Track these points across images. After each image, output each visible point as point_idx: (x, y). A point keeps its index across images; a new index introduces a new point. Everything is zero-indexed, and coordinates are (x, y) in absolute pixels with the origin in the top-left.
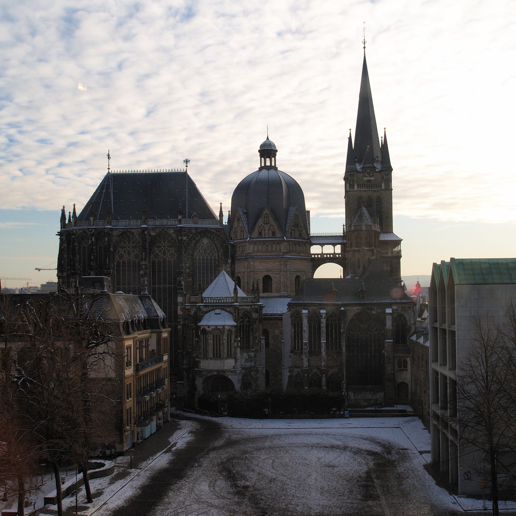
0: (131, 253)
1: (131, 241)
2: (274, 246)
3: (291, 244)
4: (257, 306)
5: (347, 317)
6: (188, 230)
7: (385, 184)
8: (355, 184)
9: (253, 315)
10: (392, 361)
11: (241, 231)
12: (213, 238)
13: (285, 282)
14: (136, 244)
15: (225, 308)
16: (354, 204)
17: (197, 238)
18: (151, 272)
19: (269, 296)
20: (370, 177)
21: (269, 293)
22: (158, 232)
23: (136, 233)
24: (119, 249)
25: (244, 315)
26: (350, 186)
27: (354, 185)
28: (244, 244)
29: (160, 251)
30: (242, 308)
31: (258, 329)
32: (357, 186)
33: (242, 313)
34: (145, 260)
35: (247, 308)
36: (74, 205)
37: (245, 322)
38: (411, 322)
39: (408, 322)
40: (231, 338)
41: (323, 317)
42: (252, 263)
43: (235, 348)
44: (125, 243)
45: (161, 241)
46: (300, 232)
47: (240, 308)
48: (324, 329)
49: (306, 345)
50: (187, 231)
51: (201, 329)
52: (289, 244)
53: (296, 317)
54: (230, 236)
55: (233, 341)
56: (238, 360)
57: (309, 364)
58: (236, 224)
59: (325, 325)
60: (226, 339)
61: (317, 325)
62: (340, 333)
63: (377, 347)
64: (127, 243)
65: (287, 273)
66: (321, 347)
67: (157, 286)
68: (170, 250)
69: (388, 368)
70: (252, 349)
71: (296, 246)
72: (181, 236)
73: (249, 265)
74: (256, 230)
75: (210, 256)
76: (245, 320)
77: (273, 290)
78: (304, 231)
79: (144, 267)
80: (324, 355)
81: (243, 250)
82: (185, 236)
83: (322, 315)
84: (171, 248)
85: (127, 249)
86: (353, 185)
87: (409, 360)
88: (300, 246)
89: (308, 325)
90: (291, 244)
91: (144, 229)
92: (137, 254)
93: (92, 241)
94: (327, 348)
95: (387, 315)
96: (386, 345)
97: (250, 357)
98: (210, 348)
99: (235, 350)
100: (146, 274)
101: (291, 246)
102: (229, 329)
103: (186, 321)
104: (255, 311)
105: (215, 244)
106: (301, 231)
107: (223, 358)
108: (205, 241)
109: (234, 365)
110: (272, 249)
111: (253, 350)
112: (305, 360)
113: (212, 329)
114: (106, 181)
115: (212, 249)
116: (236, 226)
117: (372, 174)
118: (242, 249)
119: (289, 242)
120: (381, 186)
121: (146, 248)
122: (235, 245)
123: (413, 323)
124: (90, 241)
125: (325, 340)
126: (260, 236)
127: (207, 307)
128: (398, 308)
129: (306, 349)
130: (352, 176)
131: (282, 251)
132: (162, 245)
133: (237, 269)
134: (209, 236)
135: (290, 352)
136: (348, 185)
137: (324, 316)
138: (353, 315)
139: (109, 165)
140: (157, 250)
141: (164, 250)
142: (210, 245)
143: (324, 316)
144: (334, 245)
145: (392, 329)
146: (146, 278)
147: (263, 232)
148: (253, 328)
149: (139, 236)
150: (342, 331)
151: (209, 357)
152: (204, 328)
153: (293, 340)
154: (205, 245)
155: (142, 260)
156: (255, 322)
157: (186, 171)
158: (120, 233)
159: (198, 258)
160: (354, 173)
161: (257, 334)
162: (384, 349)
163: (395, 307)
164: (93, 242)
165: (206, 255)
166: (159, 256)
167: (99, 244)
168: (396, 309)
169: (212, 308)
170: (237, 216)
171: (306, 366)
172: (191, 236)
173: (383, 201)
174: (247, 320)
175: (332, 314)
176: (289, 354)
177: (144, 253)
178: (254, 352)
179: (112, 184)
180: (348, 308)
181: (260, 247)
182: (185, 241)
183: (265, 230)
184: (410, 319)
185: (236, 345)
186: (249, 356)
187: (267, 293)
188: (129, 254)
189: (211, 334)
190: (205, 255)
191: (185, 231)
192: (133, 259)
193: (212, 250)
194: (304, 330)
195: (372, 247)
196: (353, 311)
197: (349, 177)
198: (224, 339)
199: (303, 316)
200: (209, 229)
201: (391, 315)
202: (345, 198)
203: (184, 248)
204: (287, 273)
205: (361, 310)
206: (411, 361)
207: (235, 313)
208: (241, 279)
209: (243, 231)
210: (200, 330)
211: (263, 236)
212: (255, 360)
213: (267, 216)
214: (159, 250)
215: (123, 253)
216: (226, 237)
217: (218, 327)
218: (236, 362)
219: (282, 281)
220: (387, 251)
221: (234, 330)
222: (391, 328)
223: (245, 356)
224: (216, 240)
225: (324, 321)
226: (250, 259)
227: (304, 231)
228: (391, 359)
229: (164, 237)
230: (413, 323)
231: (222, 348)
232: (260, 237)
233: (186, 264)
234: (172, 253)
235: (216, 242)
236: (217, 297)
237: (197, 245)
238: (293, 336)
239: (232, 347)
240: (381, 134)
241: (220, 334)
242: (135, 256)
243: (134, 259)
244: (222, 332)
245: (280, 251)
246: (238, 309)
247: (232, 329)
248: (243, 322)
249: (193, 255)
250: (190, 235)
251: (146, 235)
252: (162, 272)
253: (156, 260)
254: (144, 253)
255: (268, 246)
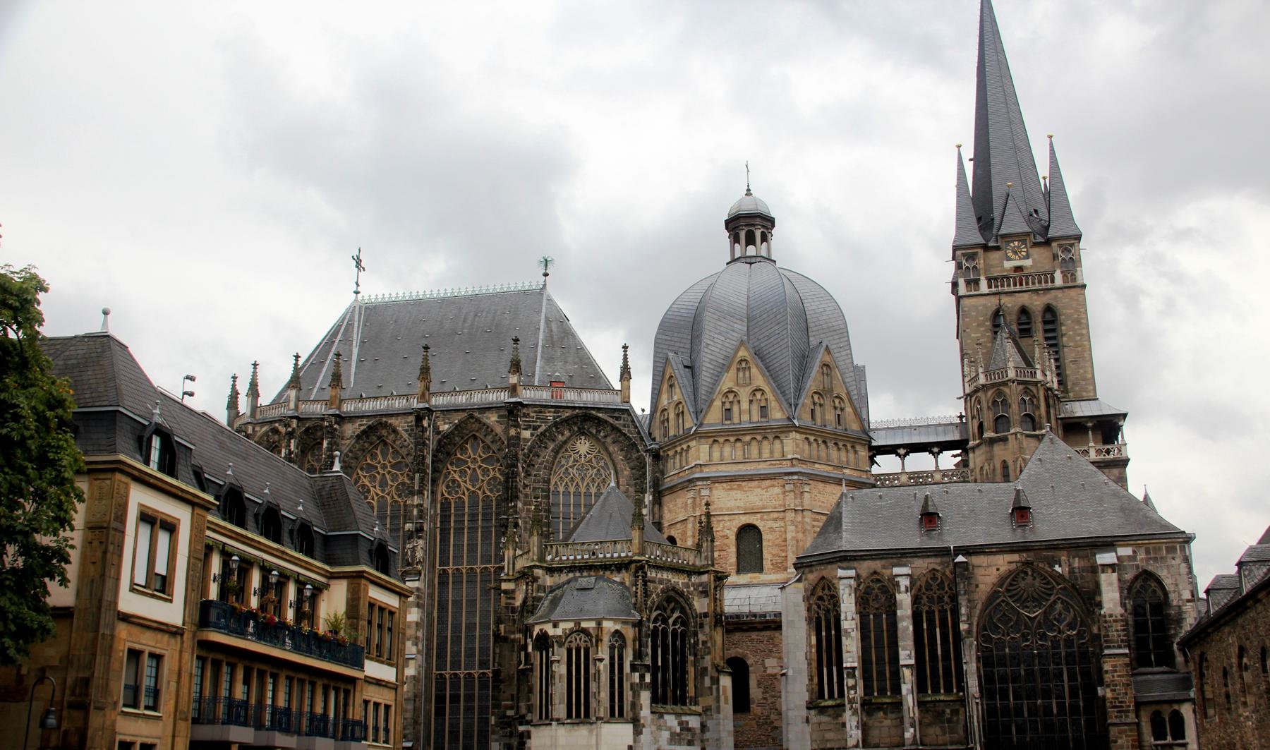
0: (390, 482)
1: (391, 451)
2: (765, 443)
3: (812, 438)
4: (706, 575)
5: (977, 586)
6: (535, 412)
7: (1062, 272)
8: (983, 278)
9: (695, 603)
10: (1132, 718)
11: (678, 415)
12: (605, 437)
13: (797, 541)
14: (403, 458)
15: (608, 573)
16: (982, 329)
17: (560, 437)
18: (438, 531)
19: (755, 581)
20: (1020, 259)
21: (757, 575)
22: (456, 421)
23: (403, 427)
24: (358, 474)
25: (669, 600)
26: (968, 282)
27: (979, 280)
28: (685, 447)
29: (463, 473)
30: (659, 575)
31: (709, 645)
32: (986, 282)
33: (659, 591)
34: (420, 492)
35: (676, 580)
36: (255, 365)
37: (671, 621)
38: (1180, 595)
39: (1172, 596)
40: (621, 658)
41: (903, 588)
42: (705, 492)
43: (636, 689)
44: (374, 456)
45: (467, 449)
46: (840, 413)
47: (654, 575)
48: (905, 624)
49: (854, 676)
50: (532, 414)
51: (535, 634)
52: (807, 438)
53: (820, 598)
54: (650, 434)
55: (627, 668)
56: (644, 726)
57: (864, 740)
58: (664, 401)
59: (909, 612)
60: (607, 661)
61: (884, 616)
62: (958, 637)
63: (1079, 680)
64: (380, 457)
65: (803, 517)
66: (902, 680)
67: (451, 568)
68: (488, 470)
69: (1120, 742)
70: (693, 708)
71: (827, 447)
72: (517, 426)
73: (698, 499)
74: (717, 403)
75: (596, 485)
76: (669, 617)
77: (767, 564)
78: (849, 410)
79: (415, 512)
80: (911, 704)
81: (684, 464)
82: (524, 429)
83: (898, 582)
84: (493, 465)
85: (378, 473)
86: (977, 282)
87: (1187, 711)
88: (839, 449)
89: (857, 617)
90: (812, 438)
91: (419, 415)
92: (403, 484)
93: (290, 450)
94: (921, 687)
95: (1103, 572)
96: (1107, 667)
97: (689, 730)
98: (559, 689)
99: (634, 697)
100: (420, 530)
101: (815, 445)
102: (617, 631)
103: (502, 627)
104: (702, 592)
105: (610, 454)
106: (842, 409)
107: (599, 719)
108: (583, 446)
109: (631, 743)
110: (760, 453)
111: (699, 709)
112: (851, 721)
113: (564, 630)
114: (348, 316)
115: (602, 467)
116: (665, 403)
117: (1027, 252)
118: (680, 461)
119: (806, 433)
120: (1053, 281)
121: (423, 464)
122: (662, 454)
123: (1189, 597)
124: (283, 451)
125: (910, 658)
126: (726, 420)
127: (556, 575)
128: (1134, 552)
129: (855, 690)
130: (971, 257)
131: (790, 457)
132: (469, 457)
133: (668, 518)
134: (594, 432)
135: (808, 708)
136: (961, 282)
137: (904, 582)
138: (995, 580)
139: (358, 285)
140: (455, 471)
141: (474, 469)
142: (595, 457)
143: (904, 582)
144: (934, 448)
145: (1122, 615)
146: (421, 542)
147: (735, 408)
148: (696, 643)
149: (410, 435)
150: (963, 627)
151: (555, 715)
152: (541, 630)
153: (815, 671)
154: (583, 457)
155: (412, 493)
156: (702, 626)
157: (545, 285)
158: (362, 428)
159: (561, 489)
160: (976, 250)
161: (707, 662)
162: (1101, 683)
163: (1125, 551)
164: (290, 452)
165: (585, 484)
166: (459, 486)
167: (309, 462)
168: (1129, 556)
169: (571, 575)
170: (667, 376)
171: (855, 744)
172: (543, 428)
173: (1063, 317)
174: (676, 615)
175: (930, 581)
176: (804, 712)
177: (417, 476)
178: (700, 715)
179: (359, 325)
180: (976, 560)
181: (727, 449)
182: (526, 440)
183: (739, 402)
184: (1177, 585)
185: (637, 681)
186: (685, 727)
187: (750, 575)
188: (383, 484)
189: (561, 645)
190: (583, 479)
191: (526, 415)
192: (393, 498)
193: (602, 471)
194: (846, 630)
195: (1041, 428)
196: (995, 568)
197: (964, 261)
198: (601, 660)
199: (841, 587)
200: (594, 412)
201: (1114, 571)
202: (957, 338)
203: (525, 462)
204: (803, 517)
205: (1019, 565)
206: (1194, 711)
207: (636, 585)
208: (678, 540)
209: (683, 412)
210: (531, 637)
211: (736, 420)
212: (702, 741)
213: (744, 364)
214: (460, 472)
215: (368, 484)
216: (639, 433)
217: (584, 625)
218: (637, 732)
219: (789, 536)
220: (1086, 449)
221: (630, 633)
222: (1119, 610)
223: (669, 724)
224: (614, 442)
225: (904, 600)
226: (698, 483)
227: (849, 410)
228: (1128, 711)
229: (475, 437)
230: (1190, 597)
231: (593, 686)
232: (729, 422)
233: (530, 505)
234: (495, 478)
235: (611, 449)
236: (583, 544)
237: (560, 455)
238: (815, 657)
239: (626, 686)
240: (1043, 170)
241: (589, 645)
242: (397, 488)
243: (396, 498)
244: (594, 640)
245: (783, 456)
246: (646, 574)
247: (623, 632)
248: (665, 621)
249: (548, 481)
250: (539, 426)
251: (424, 430)
252: (466, 531)
253: (452, 499)
254: (417, 476)
255: (749, 444)
